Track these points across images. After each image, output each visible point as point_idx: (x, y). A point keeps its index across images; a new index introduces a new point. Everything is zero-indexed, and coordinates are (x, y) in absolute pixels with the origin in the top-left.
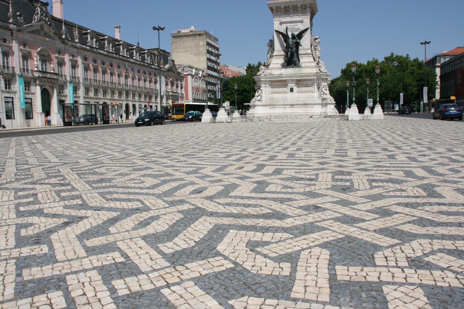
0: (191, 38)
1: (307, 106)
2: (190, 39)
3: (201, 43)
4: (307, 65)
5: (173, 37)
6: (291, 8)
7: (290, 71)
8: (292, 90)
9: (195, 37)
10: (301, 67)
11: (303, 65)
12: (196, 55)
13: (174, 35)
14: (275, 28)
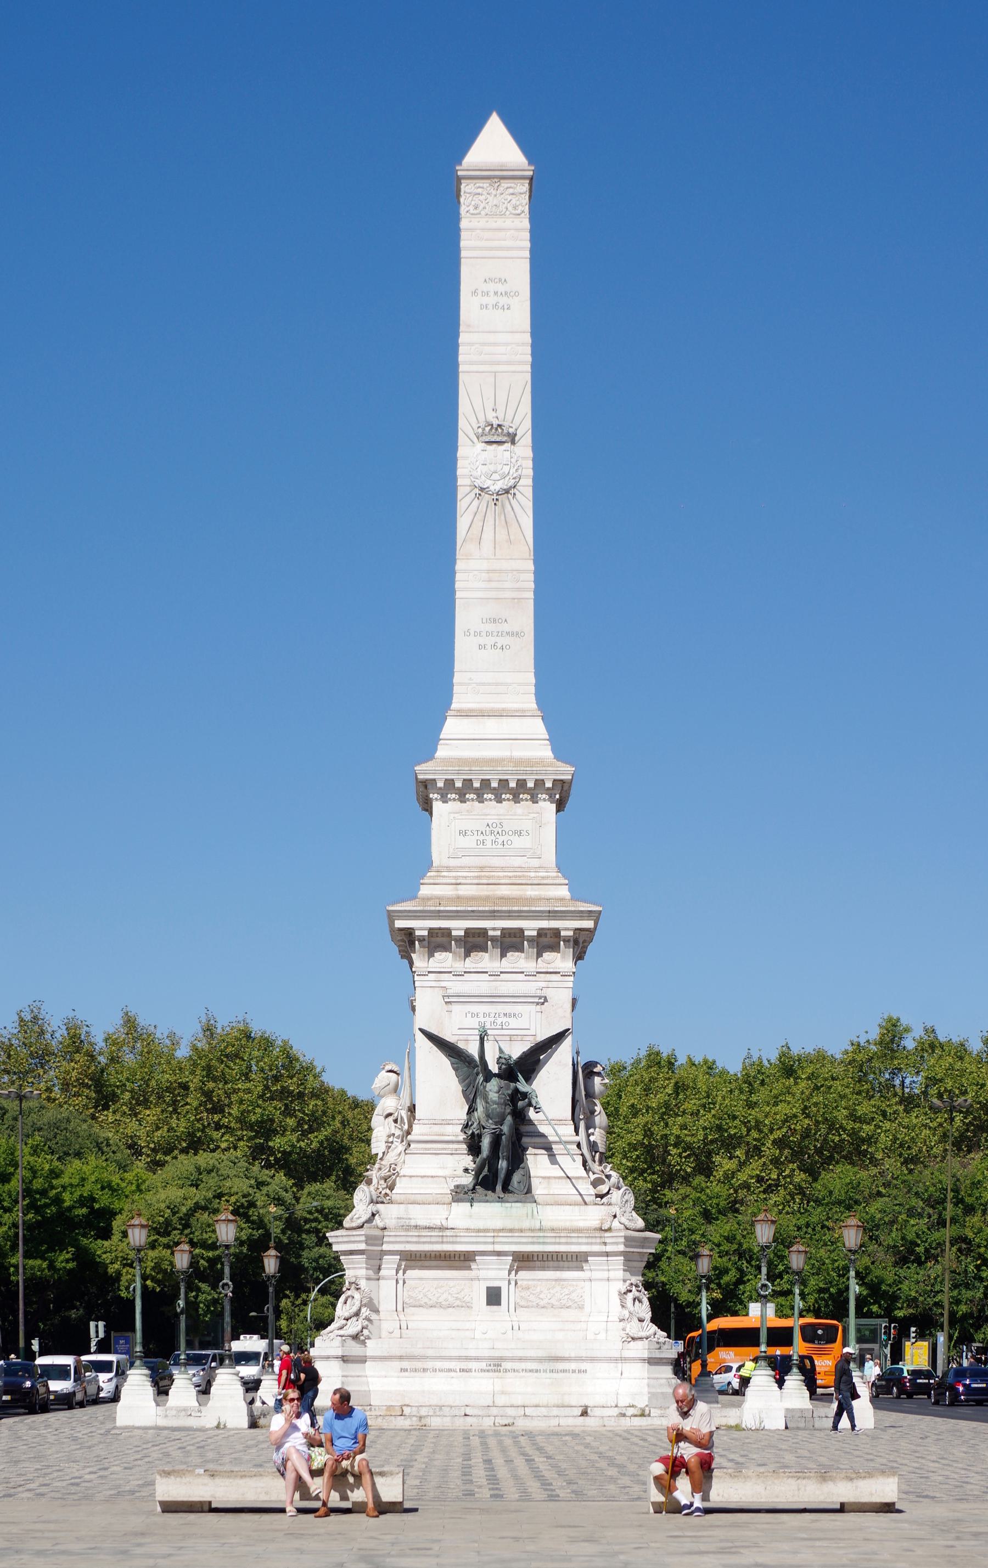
1: (561, 1366)
8: (494, 1297)
14: (422, 1020)
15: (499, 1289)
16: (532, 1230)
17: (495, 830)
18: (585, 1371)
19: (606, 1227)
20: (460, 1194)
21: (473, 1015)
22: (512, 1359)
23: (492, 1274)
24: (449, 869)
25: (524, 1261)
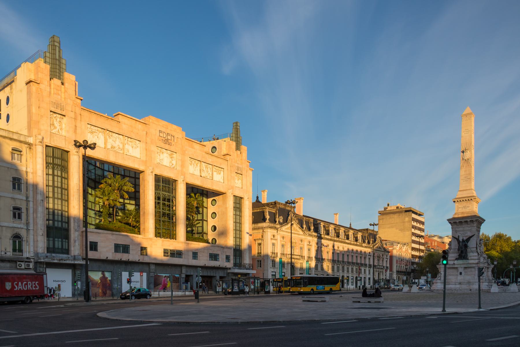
0: (398, 214)
2: (396, 216)
3: (407, 219)
4: (472, 258)
5: (380, 214)
6: (463, 222)
7: (460, 262)
8: (461, 273)
9: (401, 214)
10: (468, 259)
11: (469, 258)
12: (401, 230)
13: (381, 213)
15: (461, 272)
16: (467, 264)
17: (464, 207)
18: (474, 284)
19: (478, 263)
20: (457, 259)
21: (460, 233)
22: (463, 282)
23: (460, 270)
24: (457, 213)
25: (465, 268)
